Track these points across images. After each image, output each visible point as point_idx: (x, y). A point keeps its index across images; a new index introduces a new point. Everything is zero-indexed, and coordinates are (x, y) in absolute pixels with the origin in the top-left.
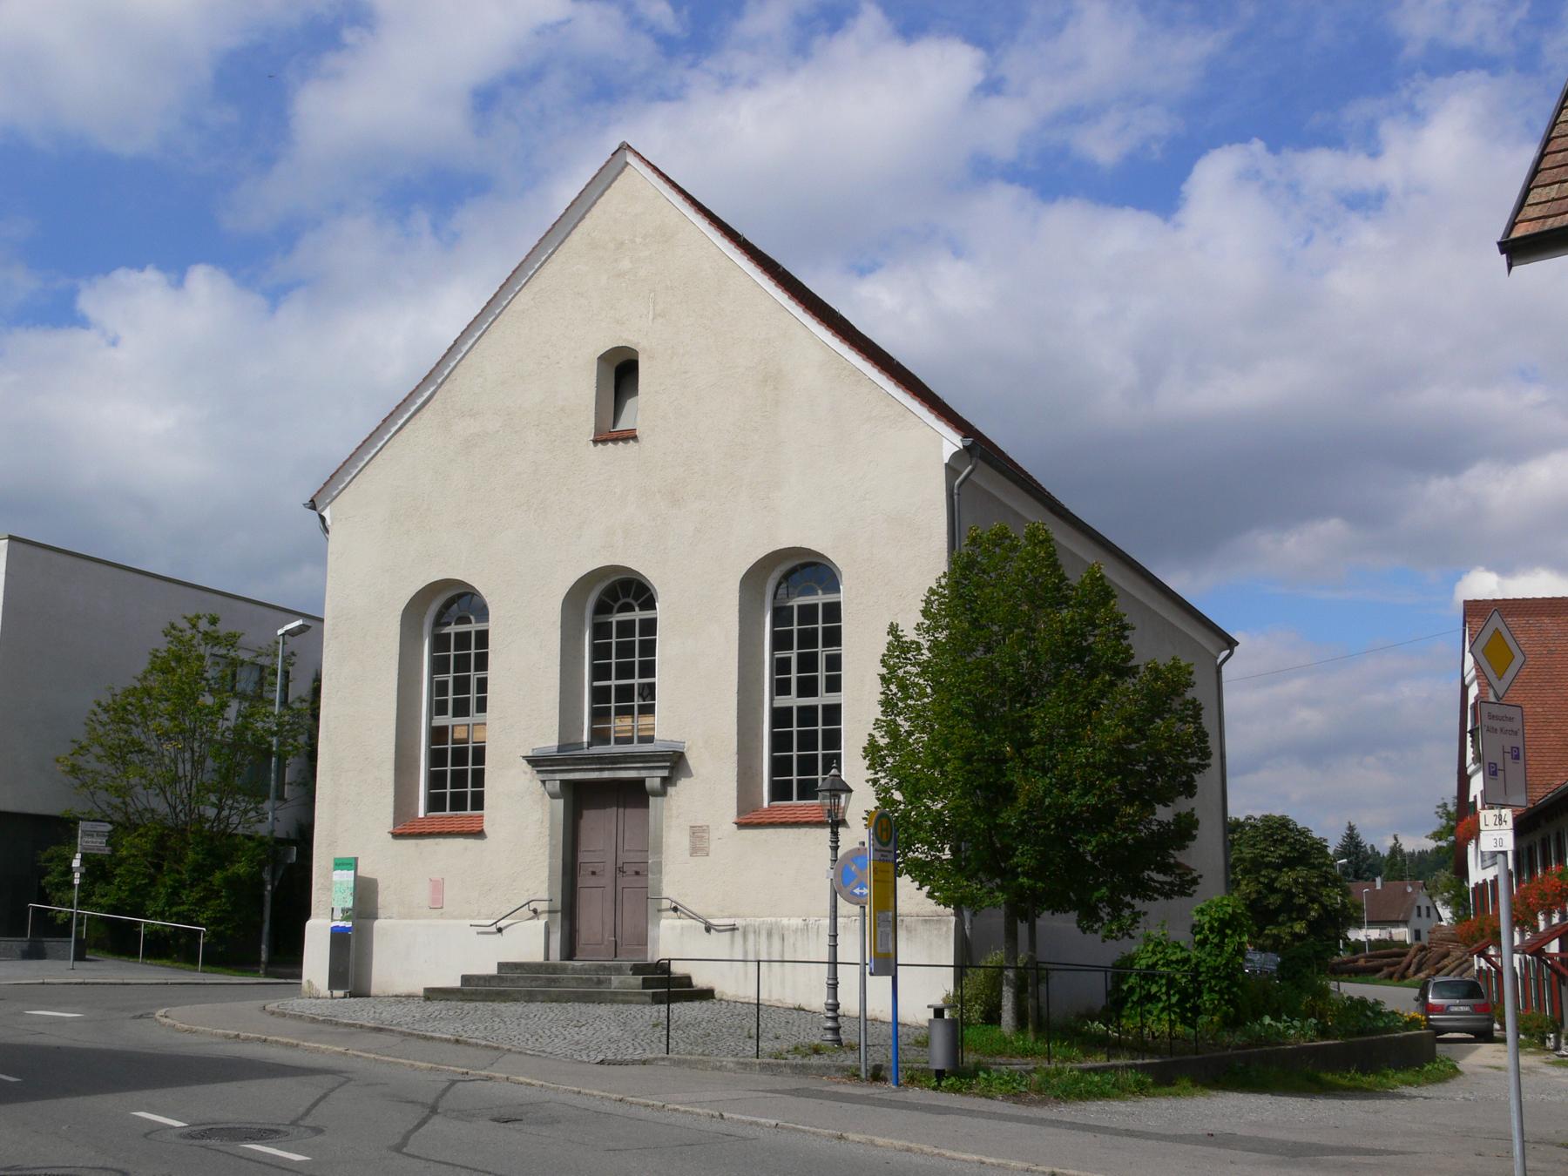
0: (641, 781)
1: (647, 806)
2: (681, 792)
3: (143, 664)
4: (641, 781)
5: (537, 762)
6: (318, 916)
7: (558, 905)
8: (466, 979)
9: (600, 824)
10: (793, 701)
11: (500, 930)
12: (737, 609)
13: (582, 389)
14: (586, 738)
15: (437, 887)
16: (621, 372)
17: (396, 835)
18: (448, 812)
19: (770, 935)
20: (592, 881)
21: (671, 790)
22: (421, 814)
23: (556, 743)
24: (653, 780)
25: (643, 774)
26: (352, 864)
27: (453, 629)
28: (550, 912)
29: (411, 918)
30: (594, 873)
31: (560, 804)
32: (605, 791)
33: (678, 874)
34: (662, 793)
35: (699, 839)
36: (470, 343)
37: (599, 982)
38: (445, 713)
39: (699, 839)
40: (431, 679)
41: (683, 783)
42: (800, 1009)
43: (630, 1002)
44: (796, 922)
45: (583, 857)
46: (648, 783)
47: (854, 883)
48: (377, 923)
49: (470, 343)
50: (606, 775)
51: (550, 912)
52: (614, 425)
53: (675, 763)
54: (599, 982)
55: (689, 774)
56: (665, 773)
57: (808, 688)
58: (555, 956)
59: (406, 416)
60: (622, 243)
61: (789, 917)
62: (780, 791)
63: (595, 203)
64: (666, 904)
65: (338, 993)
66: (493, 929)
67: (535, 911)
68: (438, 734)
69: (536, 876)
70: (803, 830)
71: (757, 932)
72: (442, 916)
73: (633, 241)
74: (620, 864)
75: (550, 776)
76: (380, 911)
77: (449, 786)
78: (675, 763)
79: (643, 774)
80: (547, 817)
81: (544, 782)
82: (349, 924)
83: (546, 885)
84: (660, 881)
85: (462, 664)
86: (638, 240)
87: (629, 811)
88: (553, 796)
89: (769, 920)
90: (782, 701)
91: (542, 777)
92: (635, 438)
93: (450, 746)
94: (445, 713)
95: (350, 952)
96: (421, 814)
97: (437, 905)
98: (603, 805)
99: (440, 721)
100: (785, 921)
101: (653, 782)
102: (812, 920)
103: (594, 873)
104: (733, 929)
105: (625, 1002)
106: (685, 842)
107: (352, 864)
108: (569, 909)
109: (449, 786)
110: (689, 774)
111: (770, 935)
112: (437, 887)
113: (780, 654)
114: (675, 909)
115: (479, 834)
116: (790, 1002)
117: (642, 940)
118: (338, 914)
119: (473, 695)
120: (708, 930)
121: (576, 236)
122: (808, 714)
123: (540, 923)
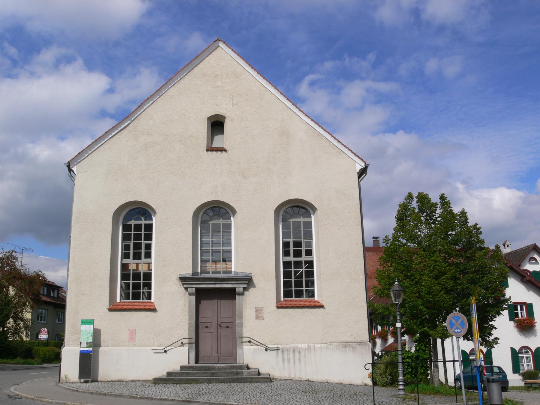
0: (234, 289)
1: (235, 299)
2: (251, 294)
3: (395, 222)
4: (234, 289)
5: (184, 280)
6: (69, 345)
7: (193, 340)
8: (169, 374)
9: (210, 307)
10: (292, 259)
11: (165, 351)
12: (273, 221)
13: (202, 129)
14: (199, 271)
15: (132, 333)
16: (217, 125)
17: (110, 310)
18: (131, 300)
19: (294, 351)
20: (207, 330)
21: (246, 293)
22: (118, 301)
23: (191, 272)
24: (239, 288)
25: (235, 286)
26: (91, 322)
27: (133, 222)
28: (189, 343)
29: (118, 346)
30: (207, 327)
31: (193, 298)
32: (215, 291)
33: (249, 326)
34: (242, 294)
35: (259, 313)
36: (148, 105)
37: (237, 374)
38: (129, 258)
39: (259, 313)
40: (122, 243)
41: (251, 290)
42: (309, 381)
43: (259, 382)
44: (305, 346)
45: (201, 320)
46: (237, 290)
47: (454, 328)
48: (101, 349)
49: (148, 105)
50: (217, 286)
51: (189, 343)
52: (211, 145)
53: (248, 281)
54: (237, 374)
55: (254, 286)
56: (245, 286)
57: (298, 254)
58: (192, 363)
59: (116, 132)
60: (217, 76)
61: (301, 344)
62: (287, 294)
63: (204, 59)
64: (245, 340)
65: (82, 380)
66: (163, 351)
67: (182, 343)
68: (125, 267)
69: (183, 328)
70: (306, 310)
71: (288, 350)
72: (135, 345)
73: (222, 75)
74: (219, 323)
75: (190, 286)
76: (102, 344)
77: (134, 289)
78: (248, 281)
79: (235, 286)
80: (187, 303)
81: (186, 289)
82: (91, 349)
83: (187, 332)
84: (242, 330)
85: (138, 237)
86: (224, 75)
87: (223, 301)
88: (190, 294)
89: (293, 345)
90: (287, 259)
91: (185, 286)
92: (225, 150)
93: (131, 272)
94: (129, 258)
95: (88, 364)
96: (118, 301)
97: (132, 341)
98: (211, 298)
99: (126, 261)
100: (300, 346)
101: (239, 289)
102: (311, 345)
103: (207, 327)
104: (278, 349)
105: (196, 383)
106: (253, 314)
107: (91, 322)
108: (196, 343)
109: (134, 289)
110: (254, 286)
111: (294, 351)
112: (132, 333)
113: (286, 240)
114: (250, 342)
115: (154, 310)
116: (304, 377)
117: (233, 356)
118: (84, 345)
119: (143, 251)
120: (266, 350)
121: (196, 70)
122: (298, 264)
123: (186, 348)
